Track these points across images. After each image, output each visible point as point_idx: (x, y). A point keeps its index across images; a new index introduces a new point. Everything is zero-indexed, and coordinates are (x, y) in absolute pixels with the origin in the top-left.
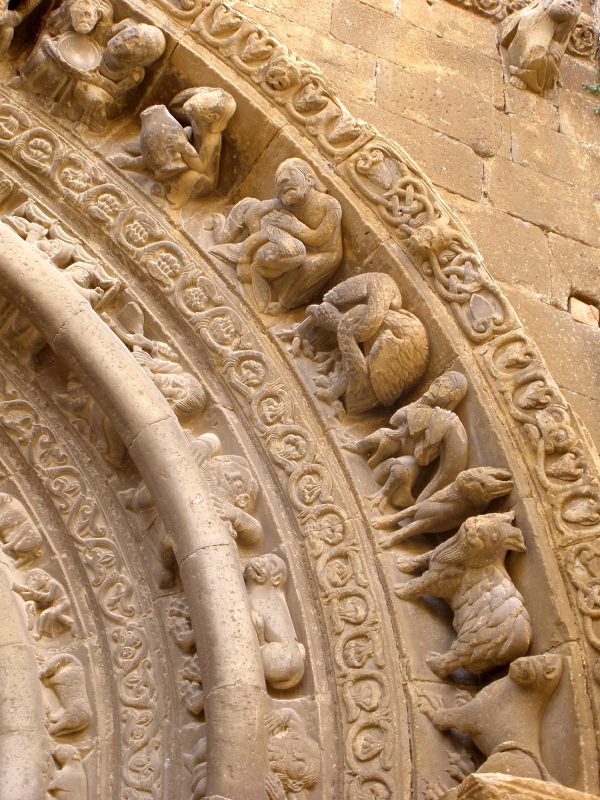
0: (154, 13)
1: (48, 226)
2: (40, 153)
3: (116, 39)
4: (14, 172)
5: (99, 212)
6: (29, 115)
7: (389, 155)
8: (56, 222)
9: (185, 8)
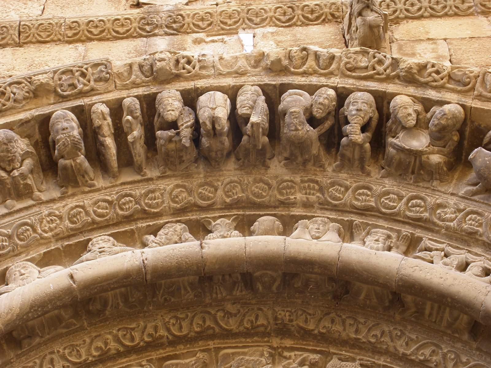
1: (443, 250)
2: (418, 208)
3: (434, 121)
4: (407, 227)
5: (470, 228)
6: (401, 189)
8: (447, 246)
9: (465, 85)
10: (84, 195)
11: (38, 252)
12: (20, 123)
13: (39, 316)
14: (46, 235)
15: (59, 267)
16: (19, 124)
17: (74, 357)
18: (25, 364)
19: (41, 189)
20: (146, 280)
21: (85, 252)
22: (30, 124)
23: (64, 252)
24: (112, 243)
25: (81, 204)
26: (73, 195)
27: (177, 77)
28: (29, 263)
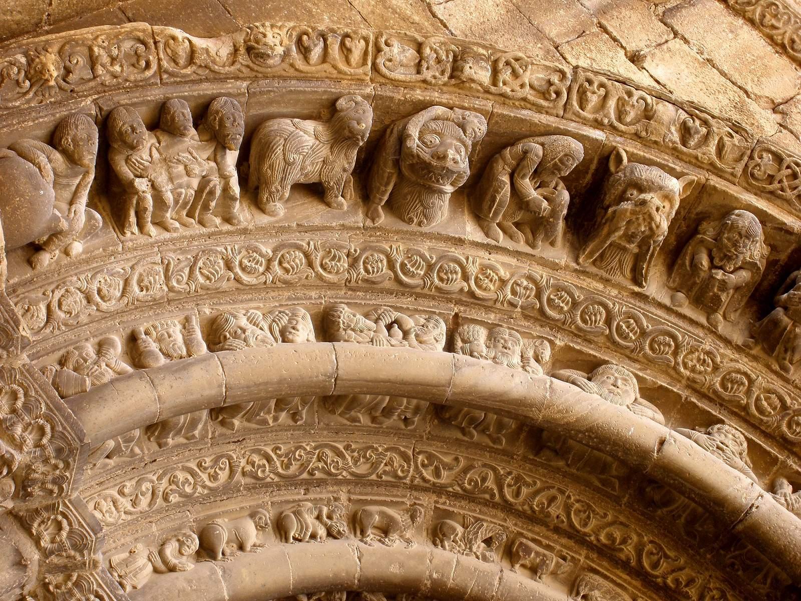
10: (766, 369)
11: (656, 378)
12: (780, 226)
13: (589, 446)
14: (682, 370)
15: (660, 416)
16: (777, 226)
17: (578, 519)
18: (525, 474)
19: (728, 316)
20: (734, 527)
21: (703, 430)
22: (788, 237)
23: (682, 405)
24: (741, 450)
25: (753, 376)
26: (755, 358)
28: (635, 380)
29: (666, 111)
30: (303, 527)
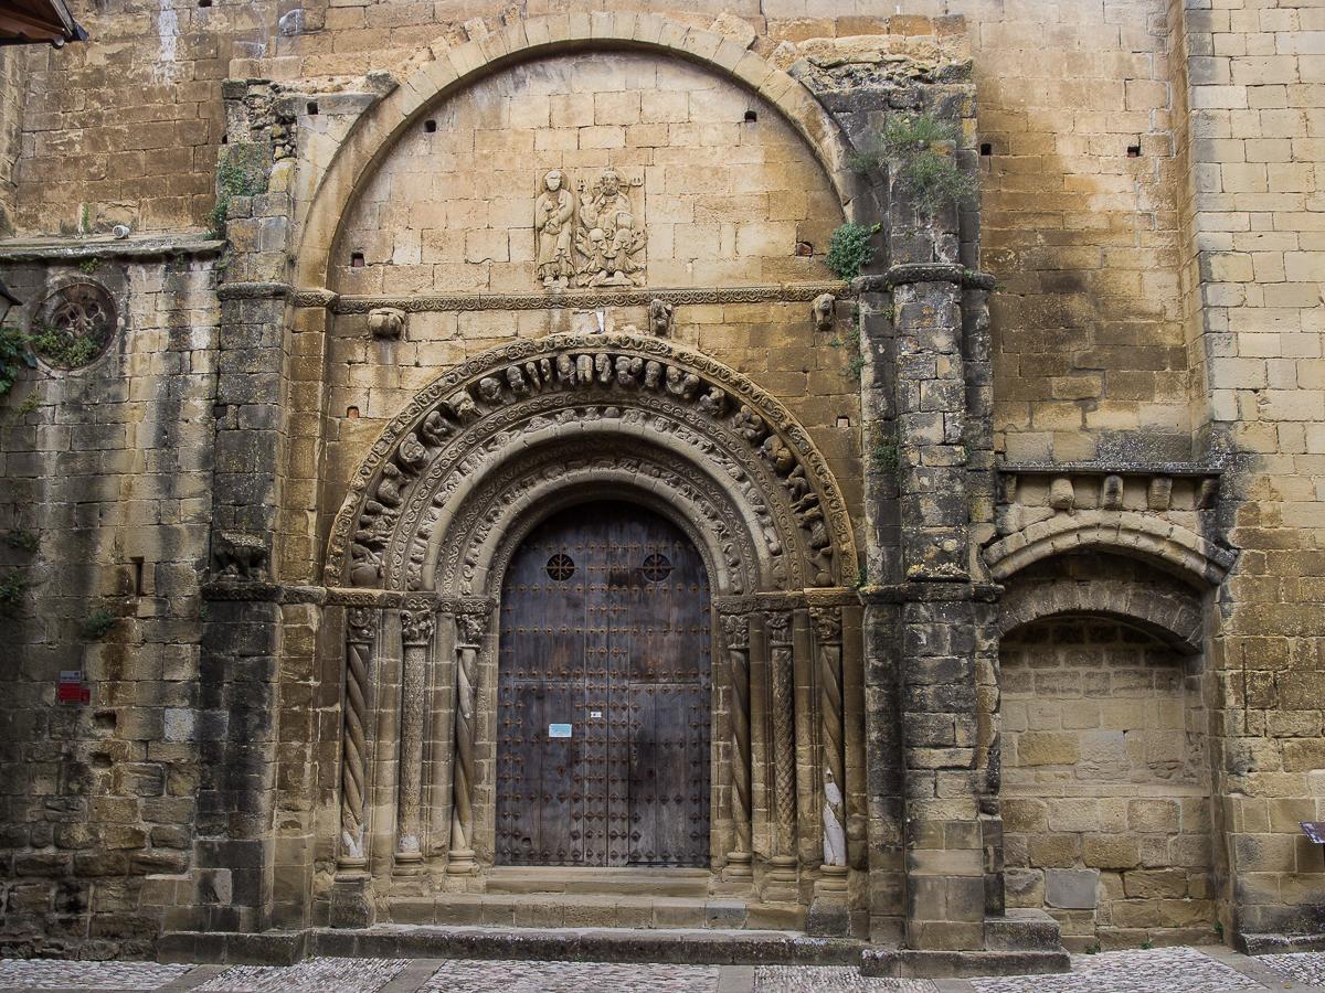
0: (694, 370)
7: (769, 400)
27: (567, 348)
29: (442, 382)
30: (482, 536)
